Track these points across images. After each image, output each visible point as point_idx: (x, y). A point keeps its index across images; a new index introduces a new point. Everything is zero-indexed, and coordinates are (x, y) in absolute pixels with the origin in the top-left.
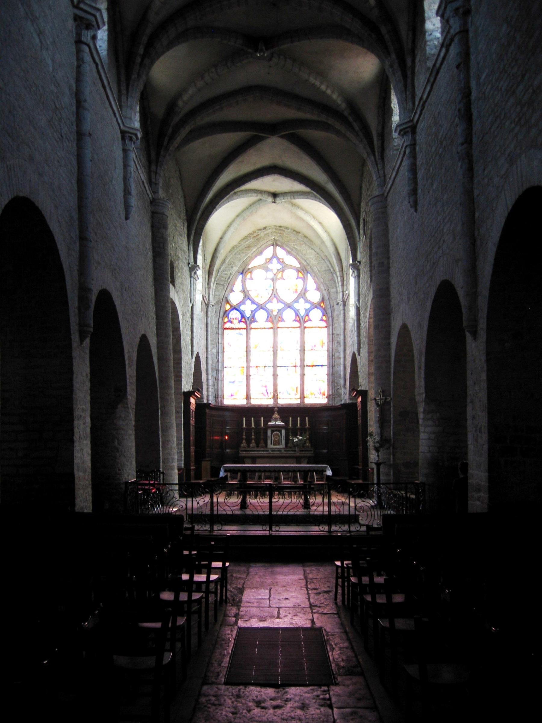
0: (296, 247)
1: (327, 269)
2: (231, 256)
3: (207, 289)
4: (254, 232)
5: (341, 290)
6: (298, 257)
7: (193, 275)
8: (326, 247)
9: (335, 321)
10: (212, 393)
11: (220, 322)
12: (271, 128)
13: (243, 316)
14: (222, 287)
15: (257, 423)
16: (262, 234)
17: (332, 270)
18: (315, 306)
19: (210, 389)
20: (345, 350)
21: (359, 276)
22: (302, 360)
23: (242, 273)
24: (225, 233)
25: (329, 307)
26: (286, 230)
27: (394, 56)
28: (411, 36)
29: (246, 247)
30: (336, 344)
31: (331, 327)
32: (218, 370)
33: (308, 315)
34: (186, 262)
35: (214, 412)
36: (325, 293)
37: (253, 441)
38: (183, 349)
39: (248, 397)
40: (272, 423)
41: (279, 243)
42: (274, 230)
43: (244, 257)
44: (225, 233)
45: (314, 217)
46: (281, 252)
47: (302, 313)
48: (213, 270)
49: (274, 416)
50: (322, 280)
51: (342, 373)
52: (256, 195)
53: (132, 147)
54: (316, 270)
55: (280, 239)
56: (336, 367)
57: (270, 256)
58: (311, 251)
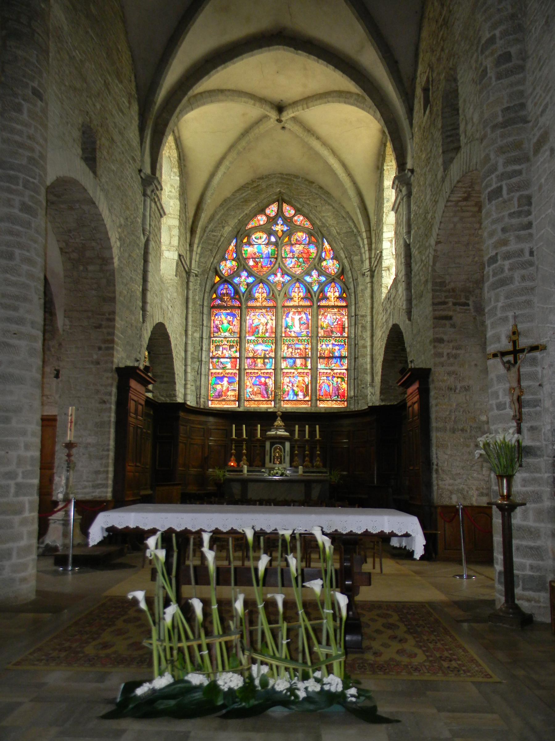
0: (308, 202)
1: (349, 230)
2: (222, 212)
3: (188, 252)
4: (253, 181)
5: (367, 256)
6: (311, 216)
8: (350, 199)
10: (192, 391)
11: (206, 298)
13: (236, 292)
14: (209, 253)
15: (251, 433)
17: (355, 230)
18: (332, 280)
19: (189, 386)
22: (314, 349)
23: (236, 237)
24: (212, 175)
25: (351, 280)
29: (242, 202)
30: (360, 329)
31: (353, 307)
32: (201, 361)
33: (322, 291)
35: (192, 417)
37: (244, 457)
39: (239, 399)
41: (286, 198)
43: (240, 214)
44: (212, 175)
45: (334, 153)
46: (289, 211)
48: (197, 227)
49: (276, 424)
50: (342, 245)
51: (369, 367)
52: (253, 102)
54: (334, 232)
57: (273, 214)
58: (327, 207)
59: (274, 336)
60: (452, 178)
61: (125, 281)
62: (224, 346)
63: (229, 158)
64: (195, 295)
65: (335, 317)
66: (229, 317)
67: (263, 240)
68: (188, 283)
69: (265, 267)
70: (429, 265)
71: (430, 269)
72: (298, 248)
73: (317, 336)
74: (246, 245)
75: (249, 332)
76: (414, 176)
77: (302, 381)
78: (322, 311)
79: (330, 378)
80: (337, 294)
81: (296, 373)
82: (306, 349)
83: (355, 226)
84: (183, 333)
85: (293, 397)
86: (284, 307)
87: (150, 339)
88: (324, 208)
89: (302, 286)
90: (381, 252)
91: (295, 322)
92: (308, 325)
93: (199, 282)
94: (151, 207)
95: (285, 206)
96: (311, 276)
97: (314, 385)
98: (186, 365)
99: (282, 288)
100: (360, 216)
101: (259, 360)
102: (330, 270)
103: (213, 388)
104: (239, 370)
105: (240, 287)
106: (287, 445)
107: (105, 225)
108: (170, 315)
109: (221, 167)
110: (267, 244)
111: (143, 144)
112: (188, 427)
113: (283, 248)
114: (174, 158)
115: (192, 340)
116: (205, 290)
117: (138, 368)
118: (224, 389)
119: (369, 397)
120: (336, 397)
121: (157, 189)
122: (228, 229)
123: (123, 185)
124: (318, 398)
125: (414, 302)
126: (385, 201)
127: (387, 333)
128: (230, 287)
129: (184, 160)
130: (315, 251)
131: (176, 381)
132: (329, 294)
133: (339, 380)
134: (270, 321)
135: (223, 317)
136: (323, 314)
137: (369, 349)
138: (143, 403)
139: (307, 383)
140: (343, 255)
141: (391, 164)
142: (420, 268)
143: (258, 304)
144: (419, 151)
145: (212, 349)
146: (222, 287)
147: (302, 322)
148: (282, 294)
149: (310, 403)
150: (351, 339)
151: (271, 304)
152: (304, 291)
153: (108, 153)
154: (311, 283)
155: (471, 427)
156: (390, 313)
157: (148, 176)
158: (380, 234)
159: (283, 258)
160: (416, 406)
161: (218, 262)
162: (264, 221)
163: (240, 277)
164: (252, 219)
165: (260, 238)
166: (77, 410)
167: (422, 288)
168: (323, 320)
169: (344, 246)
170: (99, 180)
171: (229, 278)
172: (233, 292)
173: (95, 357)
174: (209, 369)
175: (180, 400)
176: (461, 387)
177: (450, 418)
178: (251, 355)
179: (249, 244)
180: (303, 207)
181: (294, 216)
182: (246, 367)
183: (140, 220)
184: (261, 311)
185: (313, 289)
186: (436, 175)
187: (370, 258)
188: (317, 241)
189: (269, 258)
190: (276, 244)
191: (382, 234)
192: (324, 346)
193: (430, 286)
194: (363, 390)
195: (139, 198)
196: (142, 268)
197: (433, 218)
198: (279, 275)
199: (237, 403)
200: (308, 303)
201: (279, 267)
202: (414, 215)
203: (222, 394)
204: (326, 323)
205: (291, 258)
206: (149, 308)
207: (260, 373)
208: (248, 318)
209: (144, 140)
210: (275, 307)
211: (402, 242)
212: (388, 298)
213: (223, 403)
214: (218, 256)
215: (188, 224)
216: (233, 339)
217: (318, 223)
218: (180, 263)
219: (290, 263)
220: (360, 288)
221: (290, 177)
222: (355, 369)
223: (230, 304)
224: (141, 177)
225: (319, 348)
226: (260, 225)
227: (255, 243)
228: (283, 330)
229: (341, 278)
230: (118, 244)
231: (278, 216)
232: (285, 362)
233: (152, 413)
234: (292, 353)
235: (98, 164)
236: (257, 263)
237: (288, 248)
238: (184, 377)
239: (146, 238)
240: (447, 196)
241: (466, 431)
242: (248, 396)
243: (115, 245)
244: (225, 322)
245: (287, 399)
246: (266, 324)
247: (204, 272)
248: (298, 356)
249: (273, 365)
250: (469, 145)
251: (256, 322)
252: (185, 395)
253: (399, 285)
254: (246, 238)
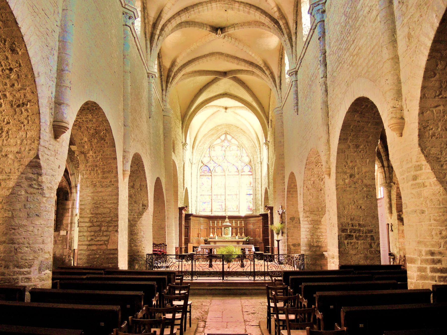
9: (256, 172)
12: (225, 74)
13: (210, 169)
16: (219, 128)
20: (261, 187)
21: (268, 149)
24: (201, 127)
27: (286, 36)
28: (295, 26)
34: (181, 141)
35: (194, 218)
36: (251, 158)
38: (179, 186)
40: (225, 224)
44: (201, 127)
46: (229, 137)
47: (240, 168)
51: (260, 198)
53: (152, 81)
54: (247, 146)
55: (228, 130)
151: (224, 174)
165: (218, 148)
175: (190, 213)
220: (257, 168)
223: (207, 174)
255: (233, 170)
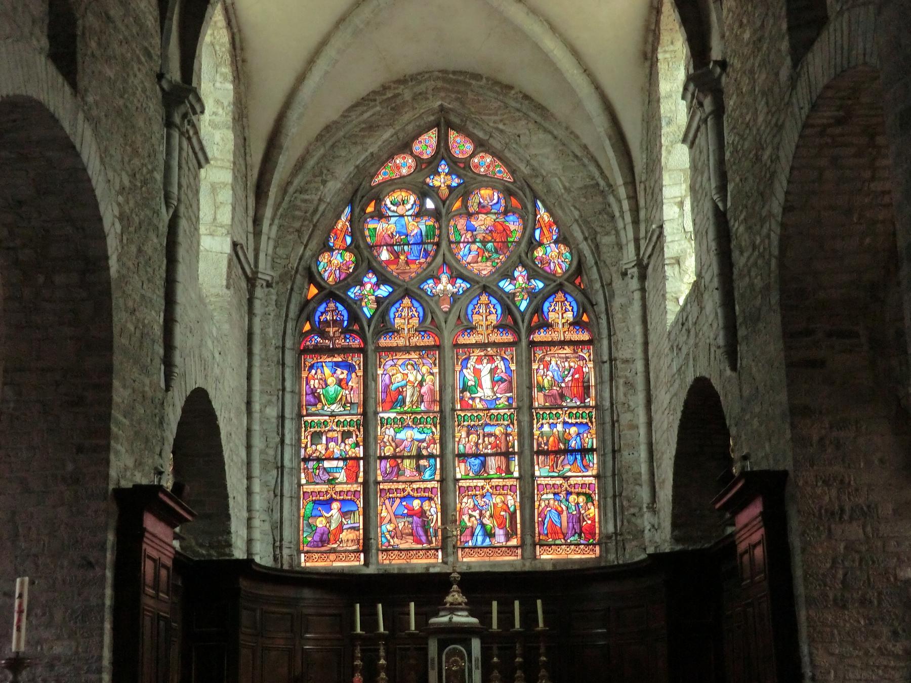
0: (501, 126)
1: (588, 182)
2: (322, 151)
3: (251, 237)
4: (385, 88)
5: (631, 235)
7: (177, 119)
8: (589, 119)
9: (618, 325)
11: (289, 331)
13: (355, 316)
15: (396, 621)
17: (602, 183)
18: (556, 287)
19: (256, 523)
22: (526, 435)
23: (351, 202)
24: (301, 79)
25: (598, 285)
26: (474, 82)
29: (362, 130)
30: (622, 389)
31: (605, 342)
32: (282, 466)
35: (265, 590)
39: (366, 547)
42: (440, 84)
44: (301, 79)
45: (553, 28)
46: (460, 146)
48: (269, 184)
49: (449, 599)
50: (576, 213)
51: (644, 469)
56: (625, 453)
58: (541, 135)
59: (437, 408)
60: (812, 79)
61: (130, 304)
62: (330, 435)
63: (337, 43)
64: (267, 327)
65: (567, 364)
66: (339, 371)
67: (408, 206)
68: (250, 302)
69: (414, 262)
70: (770, 254)
71: (774, 262)
72: (483, 222)
73: (531, 407)
74: (372, 217)
75: (383, 401)
76: (728, 75)
77: (500, 505)
78: (539, 354)
79: (562, 495)
80: (569, 316)
81: (488, 487)
82: (507, 435)
83: (602, 173)
84: (243, 407)
85: (484, 541)
86: (456, 346)
87: (180, 424)
88: (534, 138)
89: (494, 301)
90: (661, 227)
91: (483, 379)
92: (511, 382)
93: (274, 297)
94: (181, 149)
95: (453, 135)
96: (513, 279)
97: (527, 511)
98: (249, 478)
99: (452, 306)
100: (611, 153)
101: (407, 462)
102: (552, 264)
103: (309, 525)
104: (365, 484)
105: (361, 308)
106: (476, 644)
107: (93, 190)
108: (217, 371)
109: (318, 62)
110: (417, 215)
111: (167, 21)
112: (258, 612)
113: (452, 223)
114: (222, 45)
115: (262, 423)
116: (287, 316)
117: (160, 488)
118: (333, 526)
119: (647, 534)
120: (576, 536)
121: (195, 113)
122: (333, 187)
123: (126, 107)
124: (537, 539)
125: (742, 332)
126: (664, 123)
127: (683, 395)
128: (341, 308)
129: (242, 49)
130: (520, 228)
131: (231, 512)
132: (552, 316)
133: (581, 499)
134: (429, 378)
135: (327, 371)
136: (541, 360)
137: (642, 431)
138: (169, 563)
139: (512, 509)
140: (579, 235)
141: (671, 48)
142: (752, 260)
143: (401, 342)
144: (735, 27)
145: (304, 441)
146: (322, 308)
147: (496, 379)
148: (452, 319)
149: (519, 551)
150: (604, 411)
151: (429, 341)
152: (499, 311)
153: (99, 44)
154: (514, 294)
155: (880, 594)
156: (688, 354)
157: (174, 87)
158: (657, 190)
159: (450, 242)
160: (759, 552)
161: (313, 255)
162: (409, 167)
163: (362, 284)
164: (383, 164)
166: (32, 583)
167: (758, 302)
168: (541, 372)
169: (581, 216)
170: (83, 98)
171: (338, 289)
172: (346, 318)
173: (70, 467)
174: (300, 485)
175: (239, 553)
176: (852, 510)
177: (834, 577)
178: (388, 451)
179: (380, 215)
180: (491, 136)
181: (473, 155)
182: (380, 478)
183: (159, 176)
184: (407, 356)
185: (518, 308)
186: (777, 74)
187: (637, 240)
188: (524, 207)
189: (421, 243)
190: (436, 215)
191: (661, 190)
192: (546, 428)
193: (775, 298)
194: (633, 519)
195: (158, 129)
196: (164, 275)
197: (775, 159)
198: (444, 278)
199: (362, 555)
200: (509, 338)
201: (444, 262)
202: (732, 153)
203: (330, 541)
204: (549, 378)
205: (468, 243)
206: (178, 359)
207: (409, 489)
208: (380, 372)
209: (168, 14)
210: (438, 347)
211: (707, 206)
212: (682, 321)
213: (332, 556)
214: (315, 242)
215: (249, 178)
216: (348, 418)
217: (525, 169)
218: (235, 258)
219: (467, 254)
220: (618, 302)
221: (462, 78)
222: (614, 475)
223: (341, 342)
224: (162, 89)
225: (536, 433)
226: (402, 177)
227: (390, 214)
228: (458, 395)
229: (577, 282)
230: (118, 227)
231: (439, 156)
232: (462, 465)
233: (180, 583)
234: (477, 444)
235: (80, 68)
236: (397, 255)
237: (462, 223)
238: (245, 503)
239: (171, 211)
240: (804, 116)
241: (871, 602)
242: (384, 540)
243: (112, 230)
244: (331, 380)
245: (470, 544)
246: (421, 384)
247: (282, 279)
248: (489, 451)
249: (438, 472)
250: (846, 15)
251: (398, 380)
252: (250, 541)
253: (706, 296)
254: (373, 204)
255: (486, 315)
